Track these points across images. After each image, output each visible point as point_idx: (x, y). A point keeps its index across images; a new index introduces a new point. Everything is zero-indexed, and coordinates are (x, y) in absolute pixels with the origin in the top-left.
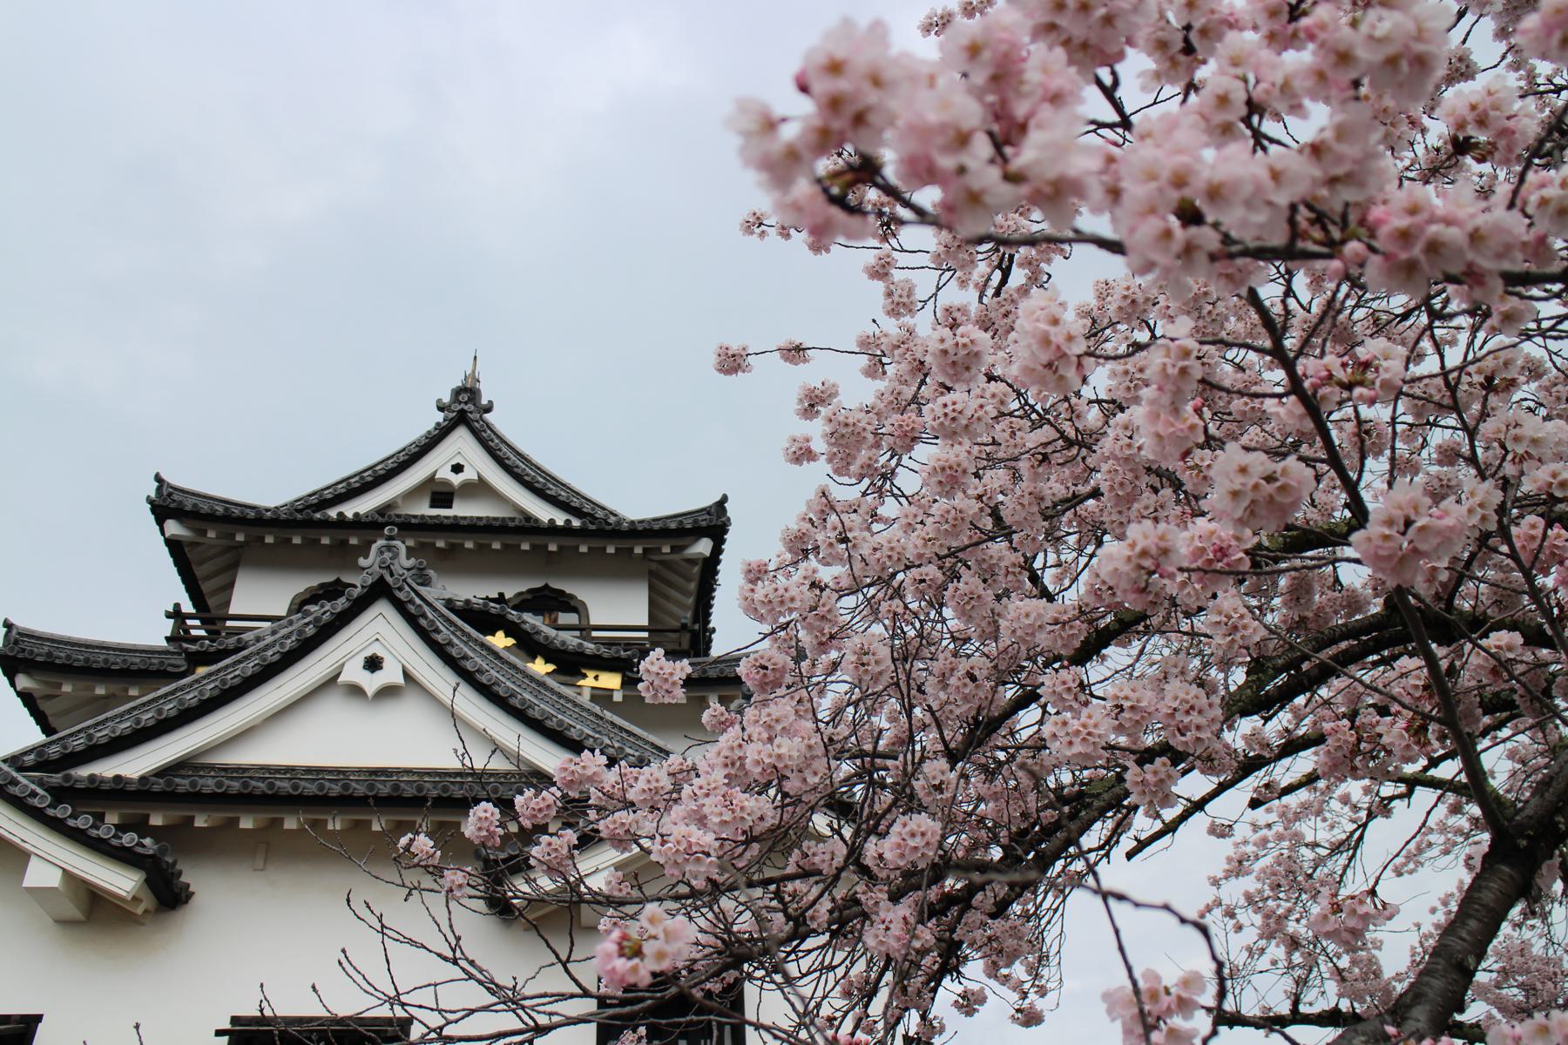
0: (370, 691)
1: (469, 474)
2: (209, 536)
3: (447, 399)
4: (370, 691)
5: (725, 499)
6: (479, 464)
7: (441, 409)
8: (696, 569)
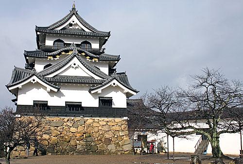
1: (75, 23)
2: (42, 33)
3: (71, 10)
6: (76, 21)
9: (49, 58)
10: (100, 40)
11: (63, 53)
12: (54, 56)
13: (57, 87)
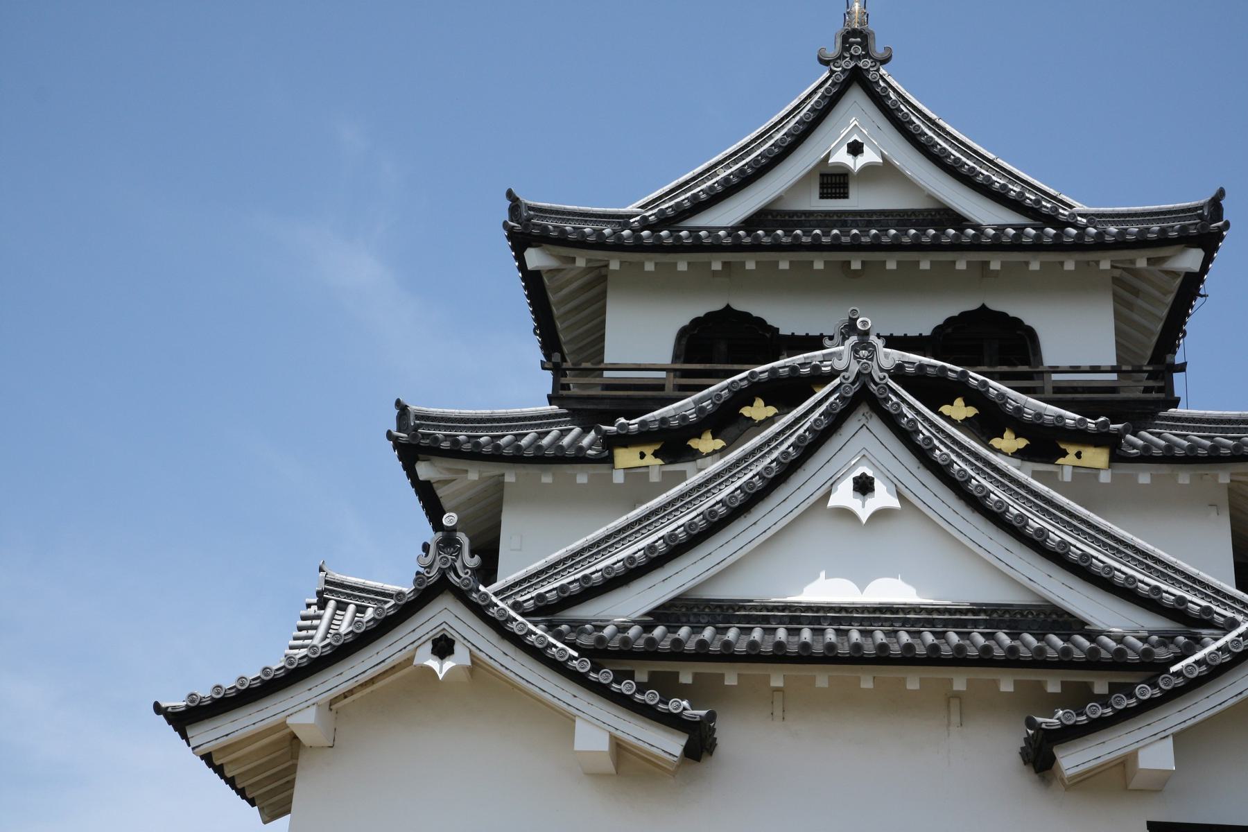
0: (864, 515)
1: (869, 156)
3: (832, 51)
4: (864, 515)
5: (1221, 193)
6: (880, 145)
7: (825, 63)
8: (1179, 281)
9: (626, 458)
10: (1125, 292)
11: (758, 410)
12: (674, 445)
13: (679, 705)
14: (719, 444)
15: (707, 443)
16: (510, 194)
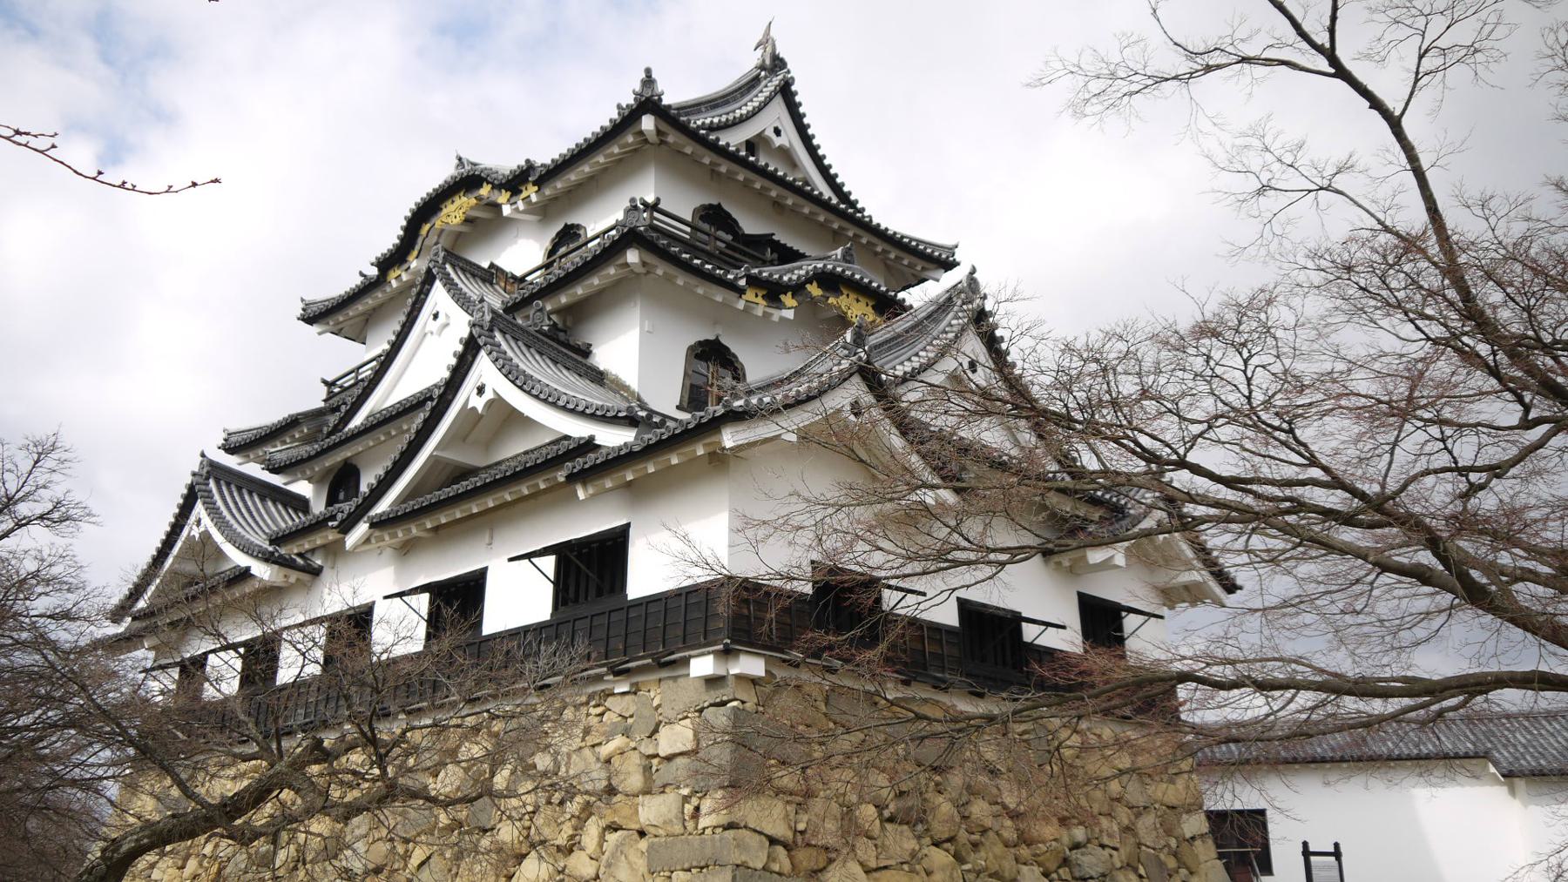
9: (750, 295)
14: (794, 303)
15: (788, 299)
16: (648, 71)
